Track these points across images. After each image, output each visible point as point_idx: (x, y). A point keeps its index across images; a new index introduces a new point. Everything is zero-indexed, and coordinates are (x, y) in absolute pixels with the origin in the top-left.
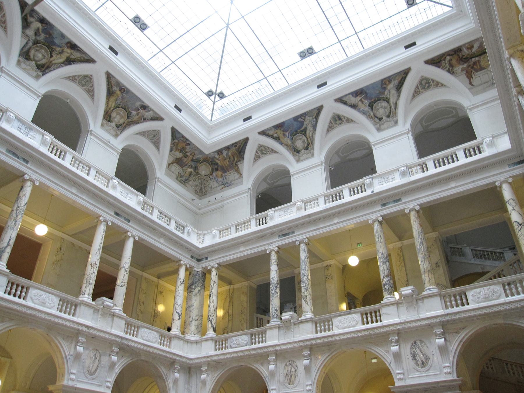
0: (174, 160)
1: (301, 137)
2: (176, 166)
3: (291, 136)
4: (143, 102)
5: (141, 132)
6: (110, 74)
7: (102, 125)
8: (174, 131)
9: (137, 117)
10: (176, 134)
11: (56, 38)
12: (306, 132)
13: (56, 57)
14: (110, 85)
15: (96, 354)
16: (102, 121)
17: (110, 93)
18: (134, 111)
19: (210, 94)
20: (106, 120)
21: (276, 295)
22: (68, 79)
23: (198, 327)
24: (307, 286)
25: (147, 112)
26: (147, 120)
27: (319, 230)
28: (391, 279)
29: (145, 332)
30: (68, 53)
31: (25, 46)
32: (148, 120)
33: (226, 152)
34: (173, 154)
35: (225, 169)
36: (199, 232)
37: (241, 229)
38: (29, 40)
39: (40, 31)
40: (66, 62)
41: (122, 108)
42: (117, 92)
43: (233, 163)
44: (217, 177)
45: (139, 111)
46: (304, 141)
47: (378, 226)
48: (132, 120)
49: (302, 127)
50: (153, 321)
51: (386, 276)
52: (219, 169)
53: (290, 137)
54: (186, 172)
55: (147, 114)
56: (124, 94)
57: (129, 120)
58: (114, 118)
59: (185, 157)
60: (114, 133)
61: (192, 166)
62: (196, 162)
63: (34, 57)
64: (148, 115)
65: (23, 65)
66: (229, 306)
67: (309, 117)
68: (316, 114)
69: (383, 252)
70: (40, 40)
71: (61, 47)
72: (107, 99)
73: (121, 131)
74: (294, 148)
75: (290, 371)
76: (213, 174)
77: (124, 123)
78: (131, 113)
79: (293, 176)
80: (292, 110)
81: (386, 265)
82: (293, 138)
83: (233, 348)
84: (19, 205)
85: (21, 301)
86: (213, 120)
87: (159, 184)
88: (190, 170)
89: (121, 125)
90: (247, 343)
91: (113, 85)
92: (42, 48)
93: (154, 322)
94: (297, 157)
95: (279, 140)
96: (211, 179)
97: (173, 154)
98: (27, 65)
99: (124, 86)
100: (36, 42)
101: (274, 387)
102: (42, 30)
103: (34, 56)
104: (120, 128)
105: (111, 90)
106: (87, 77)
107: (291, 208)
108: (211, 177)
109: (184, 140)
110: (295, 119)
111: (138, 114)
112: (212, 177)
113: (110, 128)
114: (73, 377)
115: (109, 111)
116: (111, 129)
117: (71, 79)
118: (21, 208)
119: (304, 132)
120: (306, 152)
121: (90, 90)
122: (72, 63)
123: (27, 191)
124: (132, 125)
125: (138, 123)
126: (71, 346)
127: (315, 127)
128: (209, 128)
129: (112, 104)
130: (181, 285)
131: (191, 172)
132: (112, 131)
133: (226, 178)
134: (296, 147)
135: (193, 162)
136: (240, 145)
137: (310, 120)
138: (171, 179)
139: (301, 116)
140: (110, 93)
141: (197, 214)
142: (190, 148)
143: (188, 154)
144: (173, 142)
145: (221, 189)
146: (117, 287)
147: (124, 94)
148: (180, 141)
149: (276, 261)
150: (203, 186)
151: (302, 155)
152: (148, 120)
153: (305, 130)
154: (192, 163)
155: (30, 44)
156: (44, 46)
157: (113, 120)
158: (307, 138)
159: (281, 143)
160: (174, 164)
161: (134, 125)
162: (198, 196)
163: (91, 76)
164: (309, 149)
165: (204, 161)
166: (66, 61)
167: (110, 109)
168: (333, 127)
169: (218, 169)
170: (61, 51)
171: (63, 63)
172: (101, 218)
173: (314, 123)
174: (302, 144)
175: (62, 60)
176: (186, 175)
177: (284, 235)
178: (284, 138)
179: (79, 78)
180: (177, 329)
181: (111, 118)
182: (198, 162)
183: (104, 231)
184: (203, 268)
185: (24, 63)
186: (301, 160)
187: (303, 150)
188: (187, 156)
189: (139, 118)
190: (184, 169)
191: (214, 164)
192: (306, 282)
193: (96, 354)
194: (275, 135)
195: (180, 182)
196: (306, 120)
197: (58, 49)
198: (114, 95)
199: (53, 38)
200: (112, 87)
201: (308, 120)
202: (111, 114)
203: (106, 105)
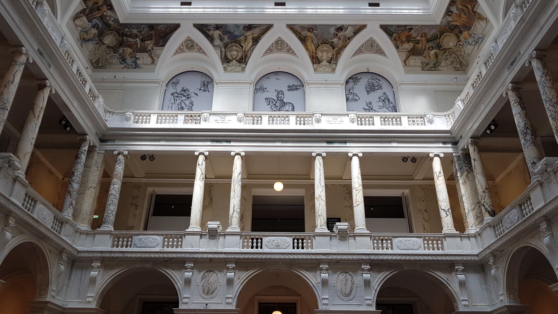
0: (408, 54)
2: (414, 58)
4: (336, 25)
5: (357, 51)
6: (291, 25)
7: (315, 70)
8: (385, 28)
9: (341, 42)
10: (389, 29)
11: (234, 31)
13: (246, 45)
14: (298, 33)
15: (346, 277)
17: (302, 40)
20: (316, 64)
22: (267, 54)
23: (477, 217)
25: (345, 31)
26: (352, 37)
29: (401, 241)
30: (250, 35)
31: (221, 54)
32: (353, 36)
34: (402, 49)
35: (467, 25)
36: (446, 113)
39: (222, 35)
40: (254, 43)
42: (308, 35)
43: (470, 13)
44: (467, 40)
45: (339, 35)
54: (430, 57)
57: (336, 49)
58: (322, 57)
59: (416, 44)
61: (432, 47)
62: (434, 40)
63: (232, 58)
64: (349, 32)
65: (229, 69)
71: (242, 35)
72: (304, 46)
73: (336, 64)
76: (461, 39)
77: (333, 55)
85: (259, 250)
87: (402, 86)
88: (433, 52)
89: (332, 58)
91: (299, 32)
92: (232, 46)
96: (462, 46)
97: (402, 49)
98: (231, 67)
99: (309, 25)
100: (226, 46)
102: (222, 33)
104: (333, 62)
105: (302, 37)
106: (277, 42)
108: (461, 43)
109: (403, 28)
111: (339, 39)
112: (462, 43)
114: (326, 301)
115: (314, 54)
116: (325, 69)
117: (269, 52)
118: (235, 179)
122: (258, 40)
123: (237, 164)
124: (341, 51)
125: (346, 46)
126: (317, 275)
129: (312, 47)
130: (438, 179)
131: (436, 53)
132: (327, 69)
133: (475, 34)
135: (431, 42)
140: (303, 40)
142: (415, 32)
143: (418, 38)
144: (393, 38)
148: (399, 32)
150: (460, 58)
152: (353, 37)
154: (430, 44)
155: (223, 50)
157: (322, 60)
160: (410, 58)
163: (280, 38)
165: (442, 33)
166: (253, 42)
167: (313, 52)
169: (461, 30)
170: (245, 38)
175: (251, 44)
179: (274, 47)
182: (437, 38)
185: (228, 66)
188: (419, 40)
189: (343, 42)
190: (424, 55)
191: (454, 28)
193: (346, 277)
195: (429, 70)
197: (242, 38)
198: (307, 39)
200: (301, 34)
202: (317, 56)
203: (307, 52)
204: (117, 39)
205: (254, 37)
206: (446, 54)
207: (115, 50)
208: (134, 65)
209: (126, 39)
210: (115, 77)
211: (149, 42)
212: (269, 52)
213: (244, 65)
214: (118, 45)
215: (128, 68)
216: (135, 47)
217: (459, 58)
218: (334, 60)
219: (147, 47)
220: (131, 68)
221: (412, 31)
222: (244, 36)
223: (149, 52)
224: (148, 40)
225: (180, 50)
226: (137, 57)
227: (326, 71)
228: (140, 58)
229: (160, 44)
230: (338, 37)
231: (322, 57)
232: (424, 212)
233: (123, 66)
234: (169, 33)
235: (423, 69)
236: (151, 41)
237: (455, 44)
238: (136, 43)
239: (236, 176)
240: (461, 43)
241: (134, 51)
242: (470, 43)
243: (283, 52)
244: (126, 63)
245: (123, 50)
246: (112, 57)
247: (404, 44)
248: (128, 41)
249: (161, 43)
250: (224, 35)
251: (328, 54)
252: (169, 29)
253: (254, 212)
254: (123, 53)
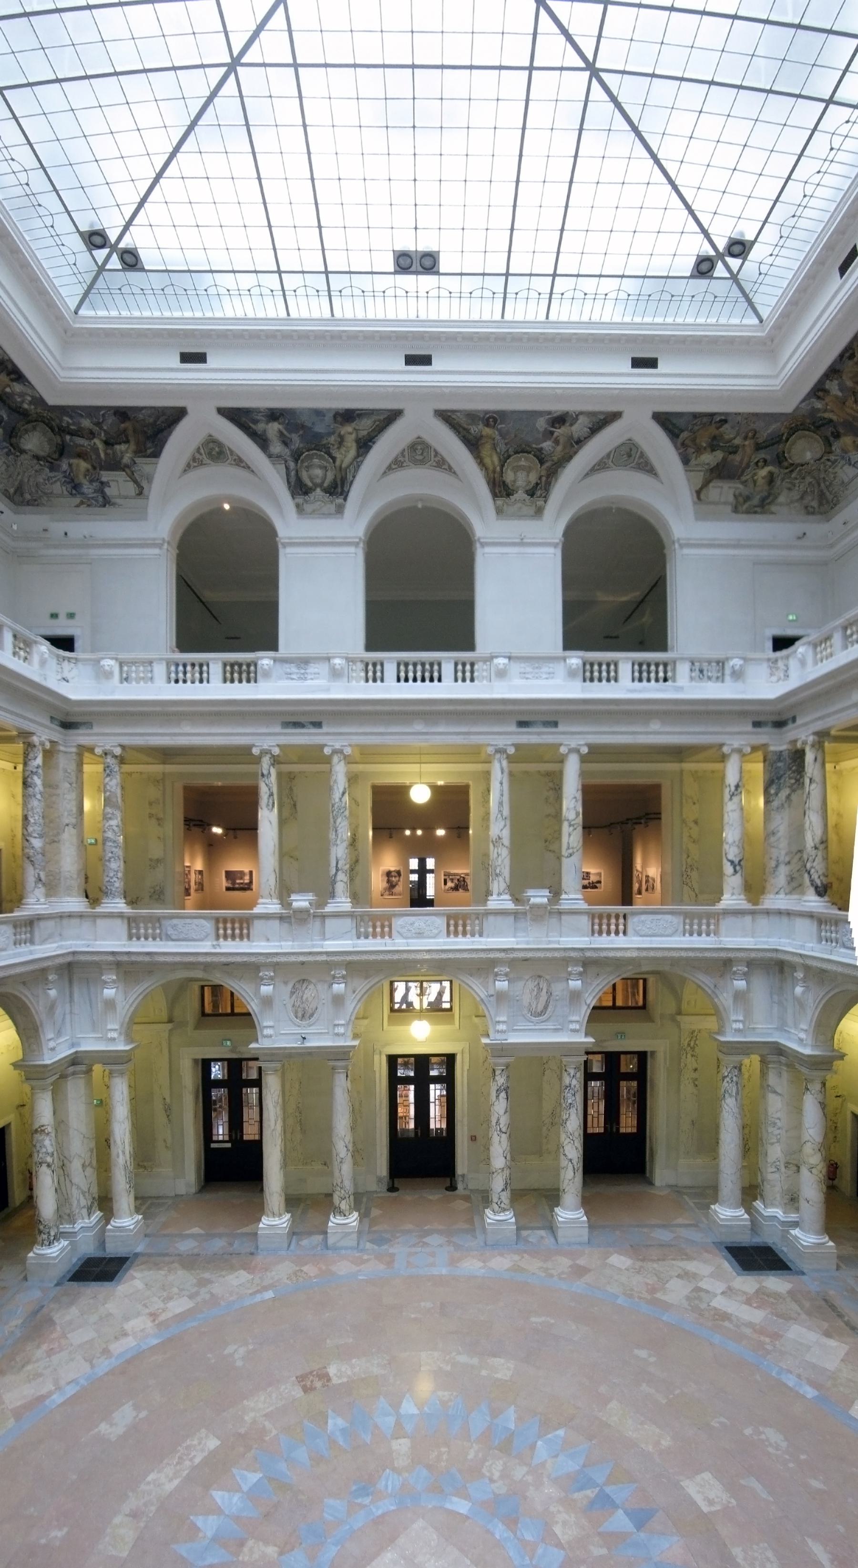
4: (549, 413)
13: (341, 454)
14: (461, 430)
16: (495, 503)
25: (571, 425)
30: (350, 433)
33: (836, 382)
38: (286, 461)
39: (285, 433)
40: (362, 450)
42: (484, 433)
56: (499, 427)
64: (579, 428)
70: (298, 449)
71: (333, 433)
76: (833, 449)
78: (541, 450)
86: (765, 317)
91: (465, 426)
99: (486, 412)
100: (297, 456)
103: (311, 479)
105: (471, 437)
108: (832, 458)
122: (370, 444)
128: (765, 344)
140: (473, 444)
147: (499, 427)
156: (312, 452)
163: (419, 438)
166: (359, 447)
171: (358, 455)
175: (353, 453)
191: (823, 425)
197: (332, 439)
199: (311, 428)
200: (468, 431)
204: (50, 441)
205: (360, 436)
207: (51, 463)
208: (101, 499)
209: (71, 440)
210: (66, 534)
211: (123, 447)
212: (394, 467)
213: (340, 501)
214: (55, 452)
215: (89, 506)
216: (94, 457)
219: (122, 458)
220: (96, 506)
222: (336, 435)
223: (127, 470)
224: (120, 443)
225: (194, 463)
226: (104, 479)
228: (111, 483)
229: (149, 451)
230: (553, 439)
233: (77, 500)
234: (165, 429)
235: (736, 510)
236: (127, 446)
238: (96, 450)
239: (337, 800)
240: (832, 458)
241: (94, 468)
244: (83, 494)
245: (70, 465)
246: (48, 480)
248: (77, 446)
249: (150, 448)
250: (290, 432)
252: (162, 419)
253: (375, 803)
254: (72, 471)
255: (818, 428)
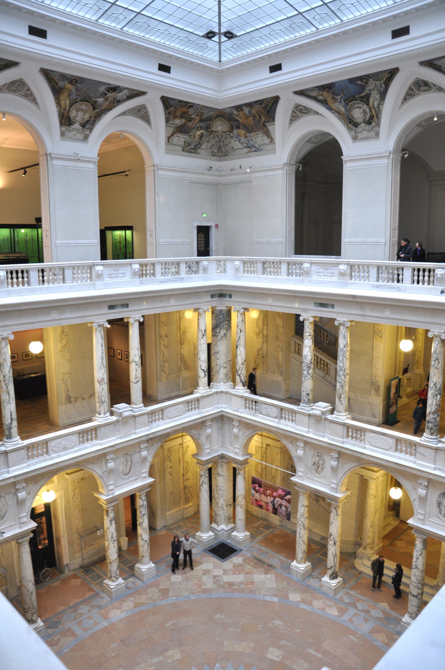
1: (360, 105)
3: (345, 101)
4: (109, 84)
7: (62, 134)
8: (165, 101)
9: (107, 103)
12: (368, 99)
15: (126, 458)
17: (57, 92)
18: (100, 98)
19: (210, 35)
20: (65, 125)
21: (310, 376)
24: (343, 383)
25: (118, 93)
26: (123, 101)
27: (364, 318)
28: (438, 416)
37: (269, 270)
41: (81, 101)
42: (66, 87)
43: (260, 123)
44: (239, 136)
45: (108, 96)
46: (365, 112)
47: (439, 345)
48: (101, 109)
49: (363, 92)
50: (181, 348)
51: (433, 413)
52: (241, 127)
53: (343, 102)
55: (119, 95)
57: (97, 110)
58: (75, 117)
59: (188, 121)
60: (81, 136)
62: (207, 121)
66: (263, 325)
67: (374, 80)
68: (387, 78)
69: (437, 381)
73: (91, 129)
74: (350, 119)
75: (318, 463)
76: (234, 131)
77: (91, 118)
79: (346, 162)
80: (346, 70)
81: (436, 400)
82: (348, 104)
83: (263, 415)
84: (4, 374)
86: (222, 60)
87: (160, 172)
88: (199, 133)
89: (88, 121)
90: (277, 416)
91: (56, 80)
93: (182, 349)
94: (353, 132)
95: (327, 104)
99: (73, 76)
101: (302, 470)
107: (333, 268)
108: (232, 135)
109: (184, 104)
110: (352, 81)
111: (106, 100)
112: (232, 135)
113: (74, 132)
115: (65, 112)
116: (75, 134)
118: (7, 377)
119: (366, 99)
120: (368, 128)
121: (28, 94)
123: (5, 353)
124: (103, 115)
127: (383, 95)
129: (65, 102)
130: (203, 338)
131: (202, 134)
133: (252, 140)
134: (353, 117)
135: (202, 123)
136: (267, 103)
137: (376, 84)
138: (174, 155)
139: (361, 78)
141: (218, 184)
142: (194, 110)
143: (193, 116)
144: (168, 111)
145: (246, 153)
146: (131, 384)
149: (310, 334)
150: (221, 143)
151: (362, 131)
153: (368, 97)
154: (201, 124)
158: (370, 109)
159: (330, 109)
160: (175, 135)
161: (106, 114)
162: (216, 157)
164: (373, 124)
165: (217, 116)
167: (65, 109)
168: (414, 94)
172: (95, 325)
173: (382, 89)
174: (362, 115)
176: (195, 140)
177: (322, 305)
178: (335, 103)
180: (204, 387)
181: (70, 119)
182: (210, 120)
183: (102, 337)
184: (227, 307)
186: (359, 138)
187: (363, 125)
188: (192, 118)
189: (110, 103)
190: (190, 134)
191: (233, 120)
192: (343, 377)
193: (126, 458)
194: (321, 98)
196: (370, 83)
198: (64, 91)
201: (372, 84)
202: (70, 115)
203: (57, 107)
206: (211, 136)
217: (220, 142)
218: (90, 123)
221: (192, 109)
227: (75, 138)
231: (75, 117)
232: (165, 338)
237: (225, 131)
242: (241, 142)
243: (16, 94)
247: (176, 119)
251: (84, 115)
255: (230, 120)
